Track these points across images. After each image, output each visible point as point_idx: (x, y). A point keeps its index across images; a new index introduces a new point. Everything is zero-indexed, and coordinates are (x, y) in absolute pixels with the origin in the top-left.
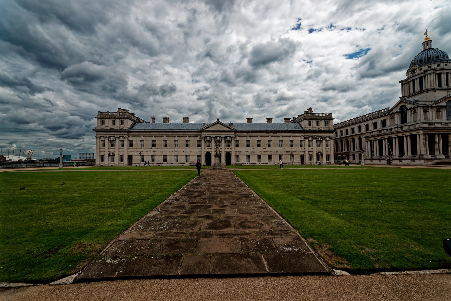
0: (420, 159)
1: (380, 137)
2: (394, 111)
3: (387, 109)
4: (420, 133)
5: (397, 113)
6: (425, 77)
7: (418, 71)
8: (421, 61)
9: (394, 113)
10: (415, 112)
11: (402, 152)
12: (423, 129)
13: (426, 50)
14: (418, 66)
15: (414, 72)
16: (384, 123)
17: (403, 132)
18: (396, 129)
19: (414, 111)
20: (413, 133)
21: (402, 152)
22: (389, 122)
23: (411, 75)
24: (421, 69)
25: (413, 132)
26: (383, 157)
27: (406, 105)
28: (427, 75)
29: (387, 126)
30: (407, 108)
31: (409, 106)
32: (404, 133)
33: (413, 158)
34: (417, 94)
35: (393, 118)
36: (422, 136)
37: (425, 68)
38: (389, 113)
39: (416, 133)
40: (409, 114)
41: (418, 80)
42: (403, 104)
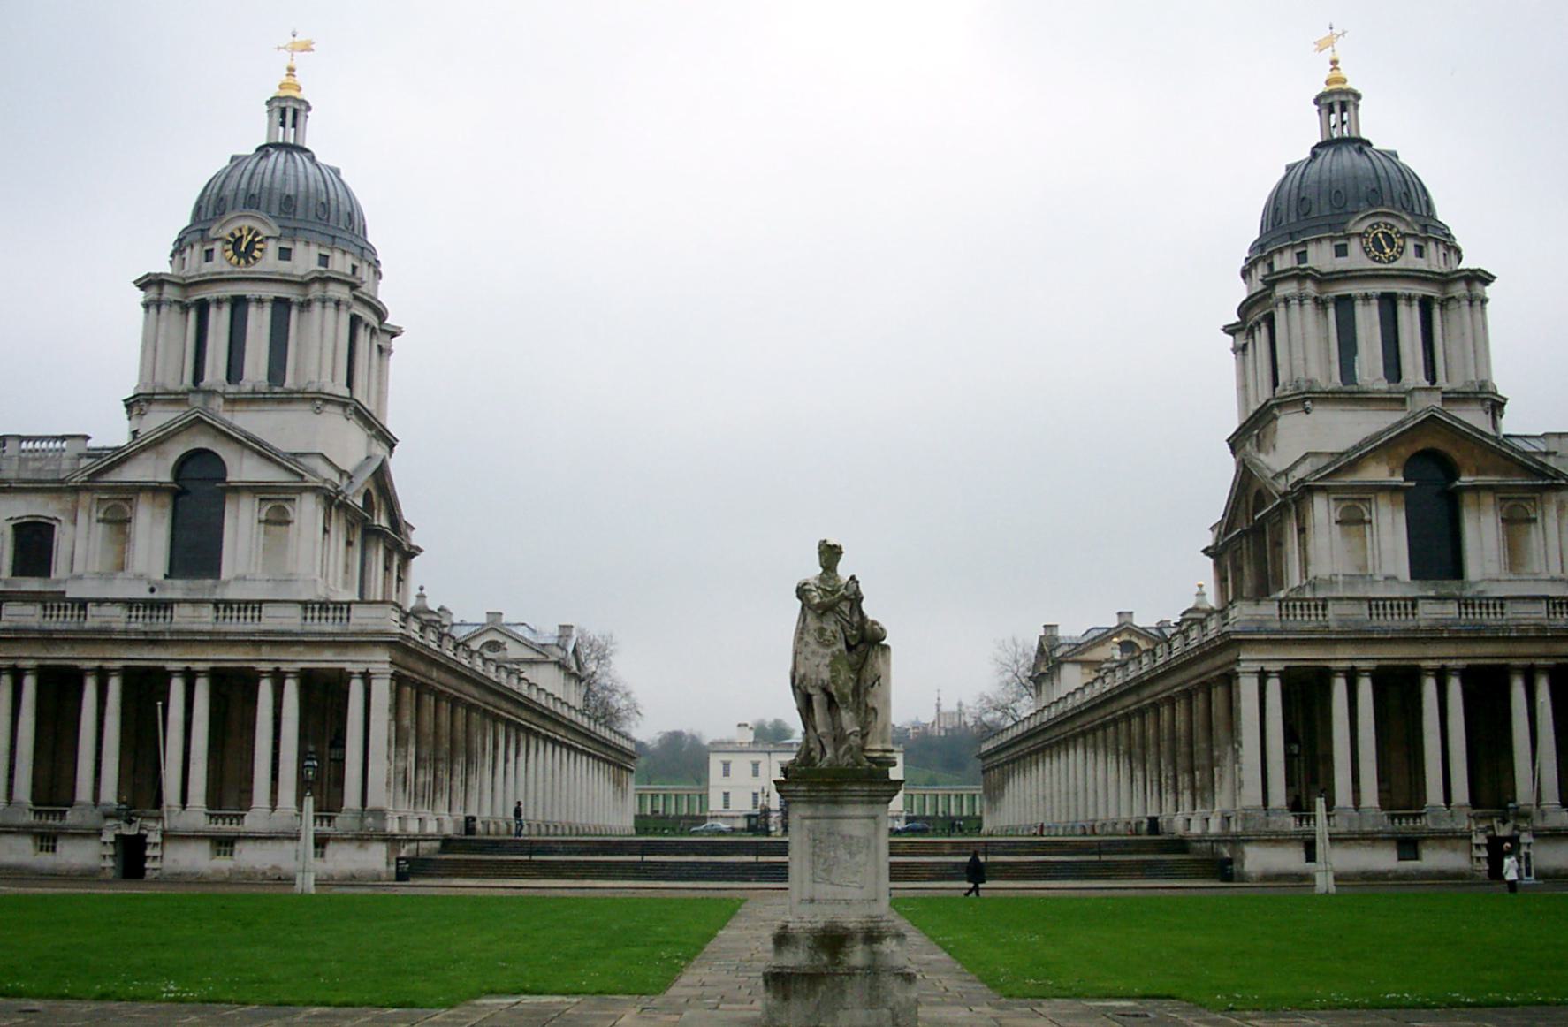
0: (362, 839)
1: (62, 655)
2: (132, 473)
3: (79, 447)
4: (373, 668)
5: (155, 489)
6: (305, 305)
7: (268, 261)
8: (288, 203)
9: (138, 489)
10: (278, 519)
11: (230, 787)
12: (399, 646)
13: (277, 146)
14: (278, 232)
15: (244, 249)
16: (34, 546)
17: (257, 644)
18: (208, 612)
19: (276, 503)
20: (325, 660)
21: (230, 787)
22: (80, 547)
23: (222, 263)
24: (285, 254)
25: (328, 655)
26: (72, 817)
27: (225, 452)
28: (324, 301)
29: (60, 568)
30: (233, 476)
31: (243, 468)
32: (266, 653)
33: (225, 827)
34: (254, 399)
35: (119, 523)
36: (382, 690)
37: (305, 260)
38: (99, 481)
39: (352, 662)
40: (241, 526)
41: (267, 310)
42: (203, 442)
